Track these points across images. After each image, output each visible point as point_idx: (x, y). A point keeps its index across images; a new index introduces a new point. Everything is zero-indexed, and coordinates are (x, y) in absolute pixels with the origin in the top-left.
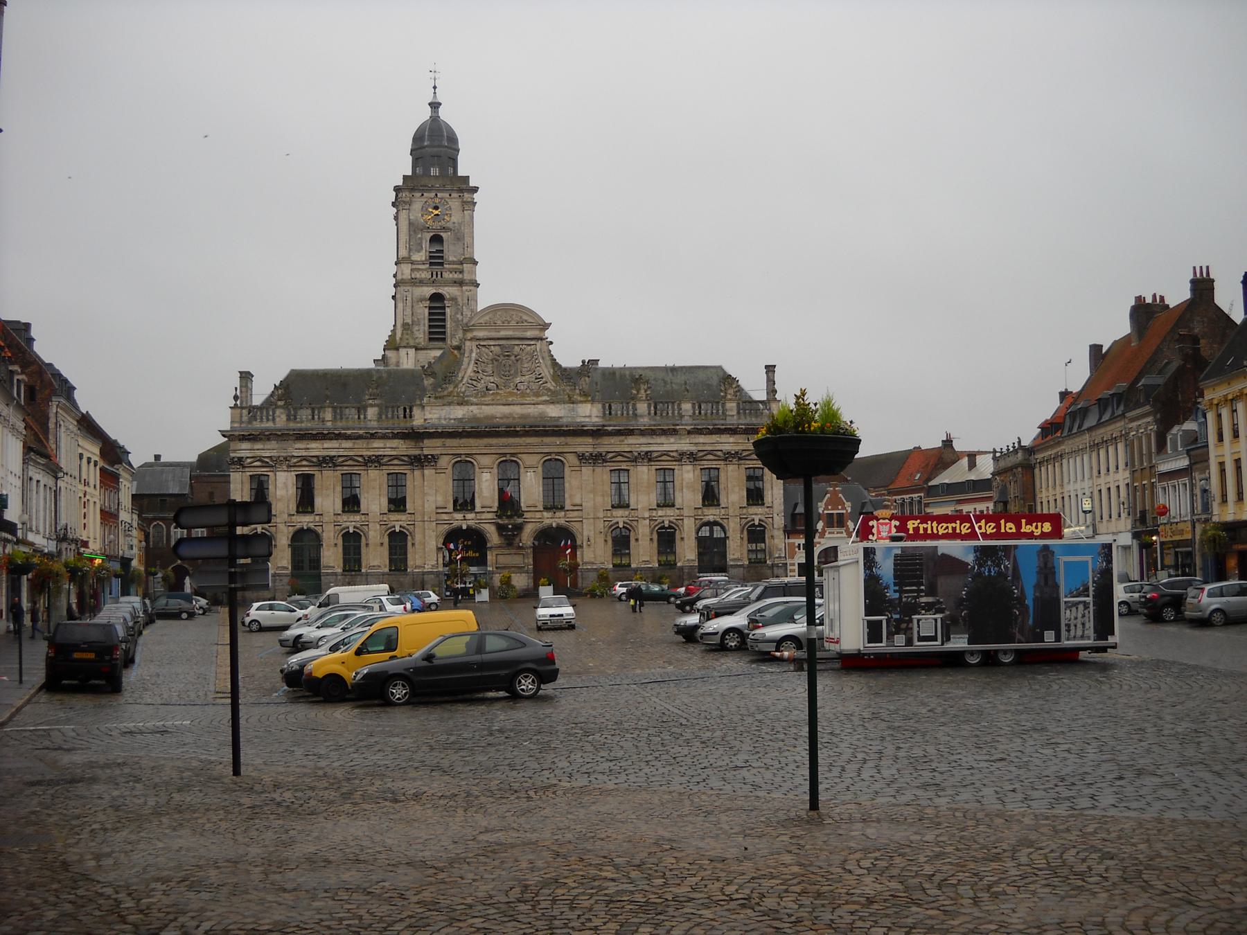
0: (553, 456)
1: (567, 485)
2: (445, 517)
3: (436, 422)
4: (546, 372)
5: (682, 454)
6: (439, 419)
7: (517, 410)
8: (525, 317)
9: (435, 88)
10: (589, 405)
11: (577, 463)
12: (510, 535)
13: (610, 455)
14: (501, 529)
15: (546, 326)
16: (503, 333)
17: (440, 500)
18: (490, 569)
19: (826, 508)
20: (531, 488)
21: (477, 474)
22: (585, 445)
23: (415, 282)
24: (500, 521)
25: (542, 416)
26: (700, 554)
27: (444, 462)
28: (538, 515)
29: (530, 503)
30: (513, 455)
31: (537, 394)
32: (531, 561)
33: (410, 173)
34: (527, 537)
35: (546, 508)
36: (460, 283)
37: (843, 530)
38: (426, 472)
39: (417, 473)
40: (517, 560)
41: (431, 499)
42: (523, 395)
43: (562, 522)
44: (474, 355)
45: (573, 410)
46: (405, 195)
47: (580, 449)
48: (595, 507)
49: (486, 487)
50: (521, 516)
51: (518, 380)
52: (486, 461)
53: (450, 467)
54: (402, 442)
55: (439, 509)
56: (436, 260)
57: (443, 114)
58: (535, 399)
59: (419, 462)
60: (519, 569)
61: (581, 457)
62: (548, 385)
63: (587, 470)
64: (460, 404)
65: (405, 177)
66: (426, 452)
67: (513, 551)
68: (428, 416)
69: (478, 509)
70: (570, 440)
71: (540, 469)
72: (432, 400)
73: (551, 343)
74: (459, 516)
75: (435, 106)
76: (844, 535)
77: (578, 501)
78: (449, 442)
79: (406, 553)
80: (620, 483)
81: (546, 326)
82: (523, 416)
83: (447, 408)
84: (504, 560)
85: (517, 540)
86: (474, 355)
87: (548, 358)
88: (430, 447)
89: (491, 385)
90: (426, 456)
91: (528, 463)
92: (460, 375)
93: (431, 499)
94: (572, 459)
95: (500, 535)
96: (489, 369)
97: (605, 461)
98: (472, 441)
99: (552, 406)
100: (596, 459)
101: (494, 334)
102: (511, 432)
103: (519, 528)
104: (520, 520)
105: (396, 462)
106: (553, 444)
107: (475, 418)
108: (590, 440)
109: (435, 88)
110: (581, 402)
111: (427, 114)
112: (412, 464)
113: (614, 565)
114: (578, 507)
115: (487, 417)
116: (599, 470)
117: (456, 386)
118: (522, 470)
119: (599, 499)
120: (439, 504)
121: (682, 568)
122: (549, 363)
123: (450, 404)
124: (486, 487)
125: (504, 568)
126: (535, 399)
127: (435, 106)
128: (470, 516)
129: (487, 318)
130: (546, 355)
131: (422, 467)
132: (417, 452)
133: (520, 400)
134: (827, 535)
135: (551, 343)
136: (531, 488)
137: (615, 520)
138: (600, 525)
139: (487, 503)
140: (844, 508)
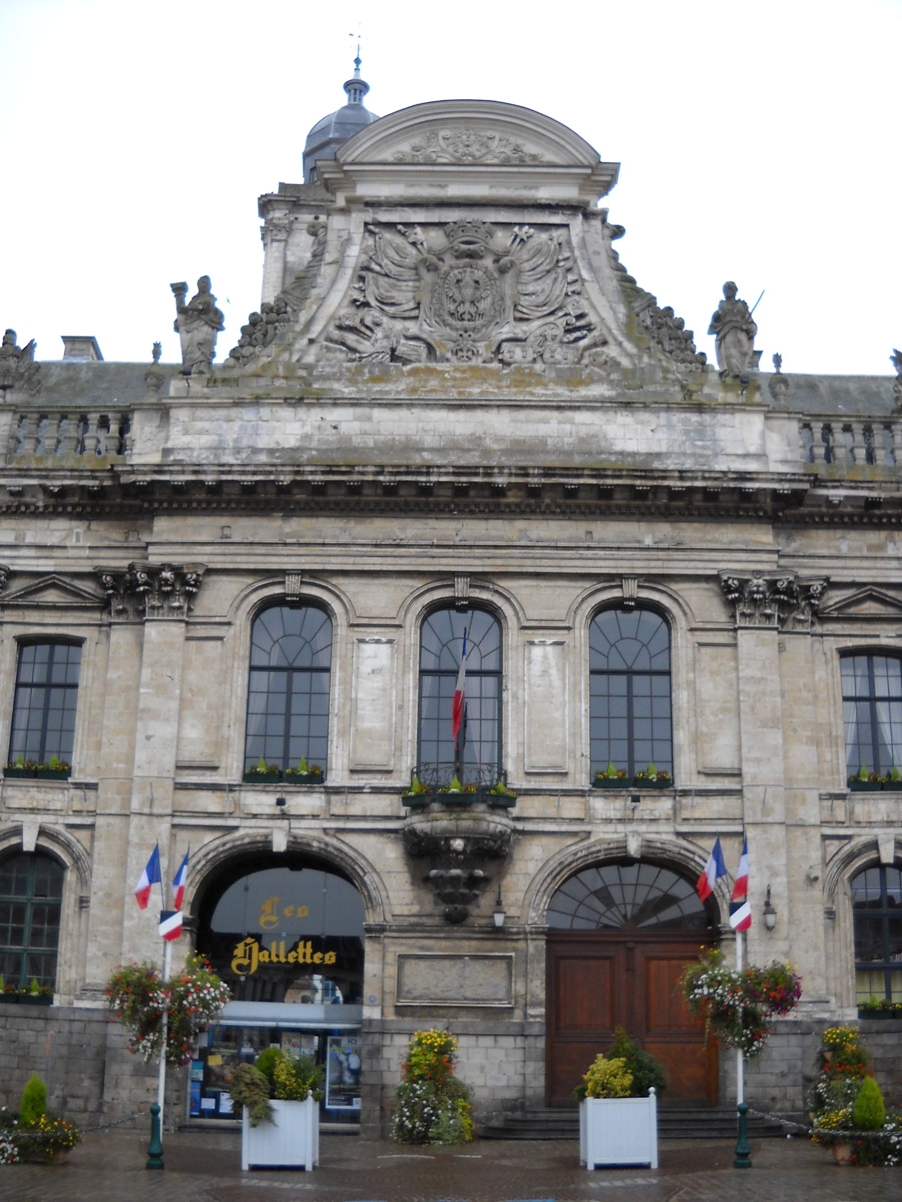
0: (631, 589)
1: (682, 697)
2: (210, 802)
3: (204, 457)
4: (605, 310)
6: (218, 448)
7: (500, 426)
8: (530, 148)
9: (358, 61)
10: (756, 421)
11: (716, 613)
12: (457, 871)
13: (836, 597)
14: (422, 852)
15: (603, 176)
16: (454, 190)
17: (195, 740)
18: (371, 1012)
20: (545, 705)
21: (339, 648)
22: (749, 550)
24: (420, 823)
25: (586, 444)
27: (222, 598)
28: (571, 807)
29: (541, 760)
30: (479, 578)
31: (571, 377)
32: (538, 987)
33: (298, 178)
34: (524, 889)
35: (603, 784)
38: (152, 631)
39: (121, 636)
40: (482, 982)
41: (163, 730)
42: (524, 378)
43: (664, 835)
44: (354, 251)
45: (701, 431)
47: (731, 565)
48: (789, 784)
49: (374, 696)
50: (502, 801)
51: (506, 331)
52: (375, 598)
53: (242, 620)
54: (79, 527)
55: (190, 776)
58: (563, 393)
59: (128, 594)
60: (491, 1018)
61: (734, 594)
62: (612, 351)
63: (756, 645)
64: (296, 401)
65: (283, 186)
66: (155, 560)
67: (468, 947)
68: (177, 438)
69: (337, 777)
70: (691, 533)
71: (581, 634)
72: (197, 387)
73: (618, 232)
74: (260, 801)
75: (356, 88)
77: (724, 759)
78: (245, 528)
79: (53, 939)
80: (872, 699)
81: (603, 176)
82: (518, 447)
83: (248, 414)
84: (429, 980)
85: (486, 901)
86: (354, 251)
87: (607, 272)
88: (173, 540)
89: (405, 347)
90: (153, 572)
91: (534, 613)
92: (303, 317)
93: (163, 730)
94: (702, 603)
95: (420, 880)
96: (404, 296)
97: (820, 616)
98: (329, 528)
99: (623, 418)
100: (789, 603)
101: (425, 192)
102: (472, 494)
103: (493, 853)
104: (497, 823)
105: (51, 596)
106: (629, 545)
107: (345, 445)
108: (764, 536)
109: (358, 61)
110: (730, 408)
112: (104, 606)
113: (866, 1012)
114: (729, 782)
115: (388, 447)
116: (799, 646)
117: (289, 347)
118: (513, 637)
119: (803, 755)
120: (194, 752)
122: (613, 285)
123: (257, 401)
124: (374, 696)
125: (430, 1011)
126: (563, 393)
128: (304, 802)
129: (404, 147)
130: (602, 261)
131: (140, 618)
132: (119, 561)
133: (511, 394)
136: (545, 705)
137: (864, 836)
138: (812, 853)
139: (375, 757)
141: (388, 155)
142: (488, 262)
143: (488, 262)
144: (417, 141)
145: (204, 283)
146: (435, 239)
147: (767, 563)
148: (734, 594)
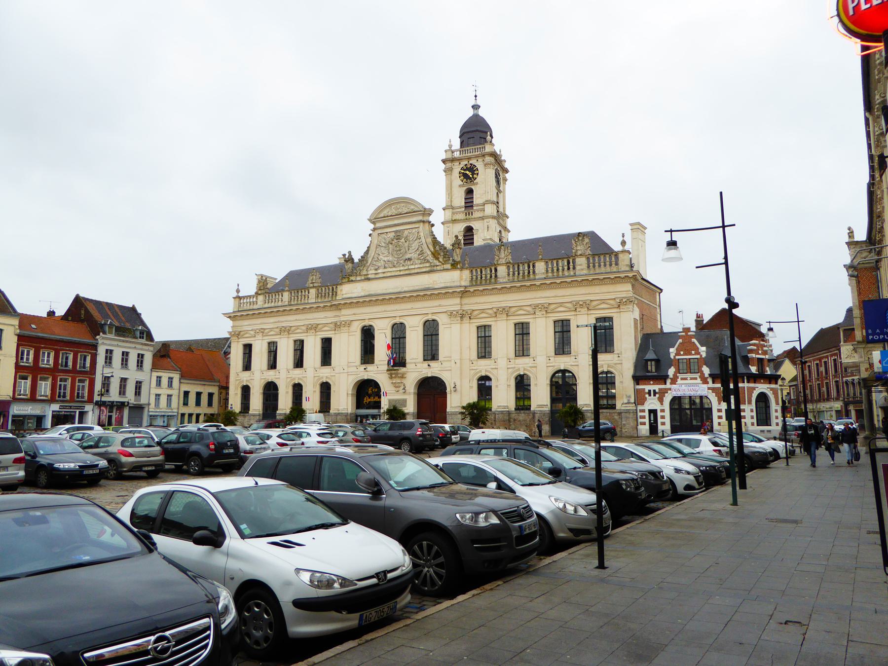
5: (536, 307)
19: (678, 354)
23: (454, 221)
26: (553, 400)
36: (482, 218)
37: (697, 376)
46: (449, 165)
56: (469, 203)
57: (481, 113)
59: (337, 326)
61: (451, 314)
63: (456, 327)
73: (433, 225)
75: (476, 107)
76: (699, 381)
88: (346, 314)
108: (457, 301)
111: (470, 113)
121: (534, 413)
122: (429, 240)
127: (476, 107)
134: (679, 381)
135: (433, 225)
140: (699, 353)
141: (382, 215)
142: (403, 240)
143: (403, 240)
144: (388, 210)
145: (350, 253)
146: (392, 235)
147: (458, 308)
148: (451, 314)
